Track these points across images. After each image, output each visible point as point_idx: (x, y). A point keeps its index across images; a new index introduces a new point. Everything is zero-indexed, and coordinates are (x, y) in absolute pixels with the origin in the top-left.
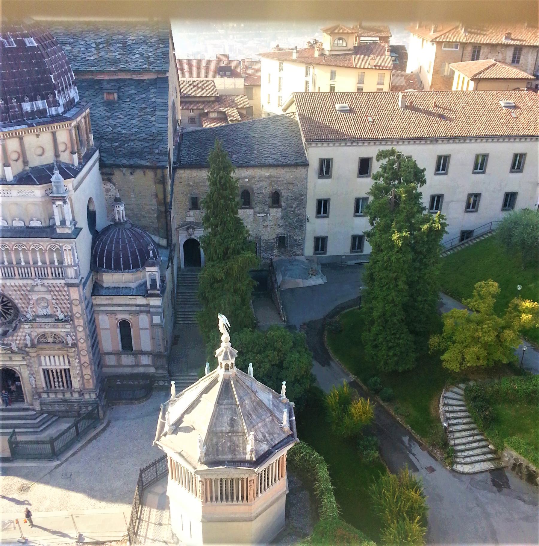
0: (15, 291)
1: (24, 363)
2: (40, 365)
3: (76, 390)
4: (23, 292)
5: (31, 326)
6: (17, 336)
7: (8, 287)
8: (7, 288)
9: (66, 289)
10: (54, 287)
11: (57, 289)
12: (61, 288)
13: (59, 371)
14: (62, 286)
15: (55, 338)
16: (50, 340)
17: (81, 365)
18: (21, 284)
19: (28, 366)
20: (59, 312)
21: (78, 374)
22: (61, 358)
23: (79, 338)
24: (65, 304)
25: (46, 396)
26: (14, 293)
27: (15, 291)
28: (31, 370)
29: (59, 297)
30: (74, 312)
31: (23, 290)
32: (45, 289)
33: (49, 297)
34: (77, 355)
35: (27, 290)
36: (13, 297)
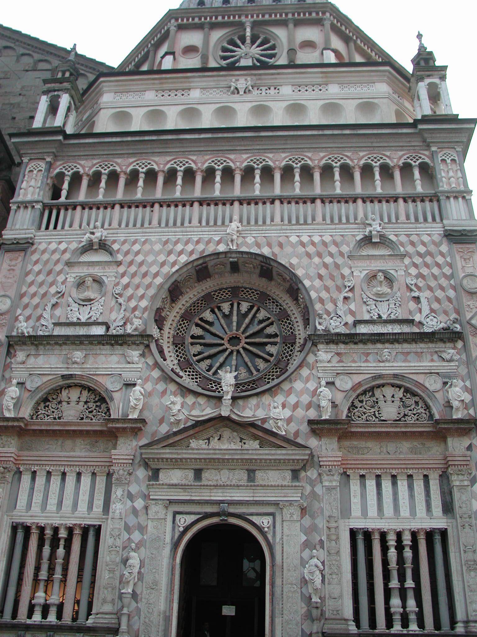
0: (309, 255)
1: (295, 496)
2: (346, 512)
4: (328, 260)
5: (336, 358)
6: (289, 392)
7: (292, 245)
8: (288, 249)
9: (444, 248)
10: (413, 244)
11: (422, 249)
12: (432, 248)
13: (407, 539)
14: (434, 243)
15: (405, 406)
18: (327, 239)
19: (303, 511)
20: (426, 310)
22: (419, 485)
24: (442, 288)
26: (305, 260)
27: (309, 255)
28: (313, 528)
29: (425, 271)
30: (468, 316)
31: (331, 255)
35: (341, 254)
36: (300, 272)
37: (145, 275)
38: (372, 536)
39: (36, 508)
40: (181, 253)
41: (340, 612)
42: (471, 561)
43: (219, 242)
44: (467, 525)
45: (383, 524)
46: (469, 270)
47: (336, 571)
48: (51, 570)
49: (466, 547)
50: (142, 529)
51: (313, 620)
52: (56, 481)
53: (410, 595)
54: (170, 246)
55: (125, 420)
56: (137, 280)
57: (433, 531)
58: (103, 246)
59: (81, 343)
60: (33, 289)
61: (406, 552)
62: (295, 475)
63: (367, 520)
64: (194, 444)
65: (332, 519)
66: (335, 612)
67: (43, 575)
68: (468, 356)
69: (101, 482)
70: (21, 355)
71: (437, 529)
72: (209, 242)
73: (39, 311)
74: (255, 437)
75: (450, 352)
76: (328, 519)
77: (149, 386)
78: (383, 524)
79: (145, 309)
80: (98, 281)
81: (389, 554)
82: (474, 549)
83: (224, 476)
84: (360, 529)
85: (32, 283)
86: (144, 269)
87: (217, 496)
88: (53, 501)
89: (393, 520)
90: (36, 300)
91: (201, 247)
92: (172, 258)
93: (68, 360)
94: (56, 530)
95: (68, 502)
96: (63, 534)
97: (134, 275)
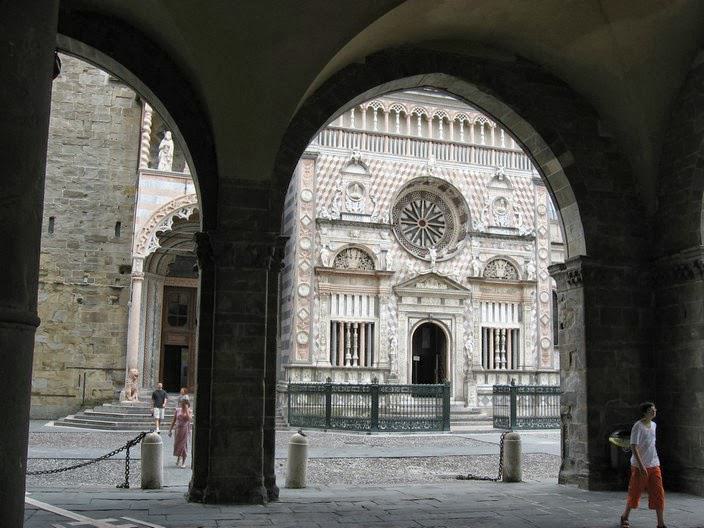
0: (468, 183)
1: (461, 312)
3: (527, 369)
4: (477, 187)
8: (457, 177)
9: (532, 187)
10: (517, 183)
11: (521, 187)
16: (501, 273)
17: (540, 322)
18: (477, 174)
19: (464, 318)
21: (533, 337)
22: (510, 308)
23: (540, 271)
25: (483, 381)
29: (522, 200)
32: (503, 186)
33: (510, 197)
34: (536, 301)
35: (483, 184)
36: (464, 193)
37: (385, 185)
39: (341, 313)
40: (403, 173)
43: (423, 169)
46: (541, 201)
48: (352, 343)
50: (396, 325)
51: (469, 366)
52: (349, 299)
53: (503, 356)
54: (397, 168)
55: (384, 271)
56: (381, 188)
58: (361, 163)
59: (358, 225)
60: (323, 187)
62: (461, 301)
64: (418, 285)
67: (349, 346)
68: (537, 249)
69: (372, 301)
70: (324, 230)
72: (418, 168)
73: (329, 202)
74: (445, 283)
75: (530, 247)
77: (393, 252)
79: (387, 207)
80: (362, 188)
83: (431, 301)
85: (321, 183)
86: (384, 181)
87: (428, 310)
88: (349, 309)
90: (326, 194)
91: (414, 171)
92: (399, 176)
93: (350, 234)
94: (352, 325)
95: (357, 311)
96: (356, 326)
97: (379, 185)
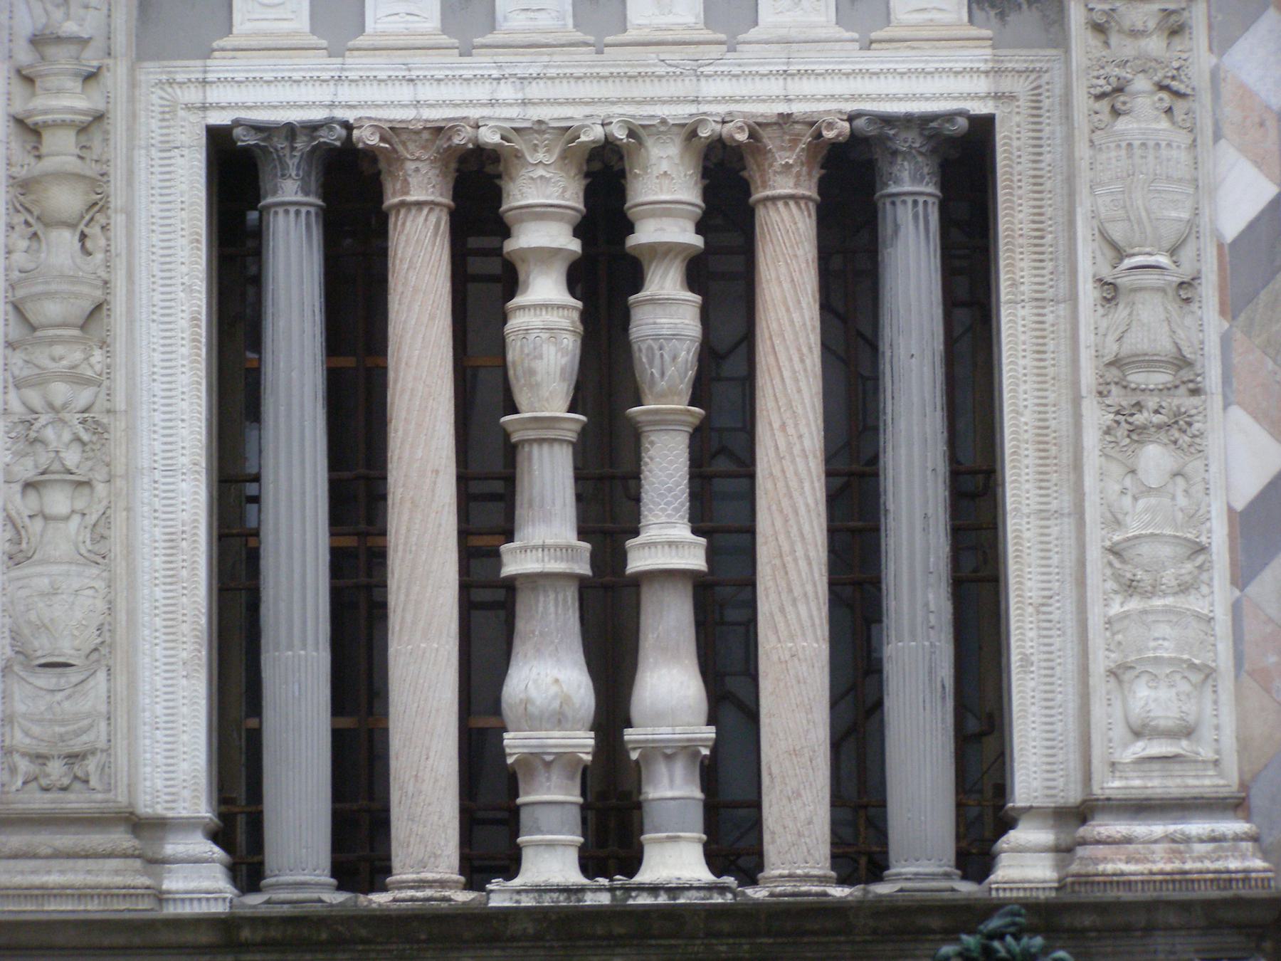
38: (389, 187)
41: (91, 765)
42: (1147, 362)
44: (1141, 84)
45: (481, 92)
47: (72, 457)
49: (1120, 253)
57: (882, 140)
61: (652, 301)
63: (352, 60)
65: (61, 57)
66: (56, 769)
71: (908, 121)
76: (24, 56)
78: (481, 92)
81: (516, 322)
82: (1186, 271)
84: (291, 131)
89: (559, 61)
